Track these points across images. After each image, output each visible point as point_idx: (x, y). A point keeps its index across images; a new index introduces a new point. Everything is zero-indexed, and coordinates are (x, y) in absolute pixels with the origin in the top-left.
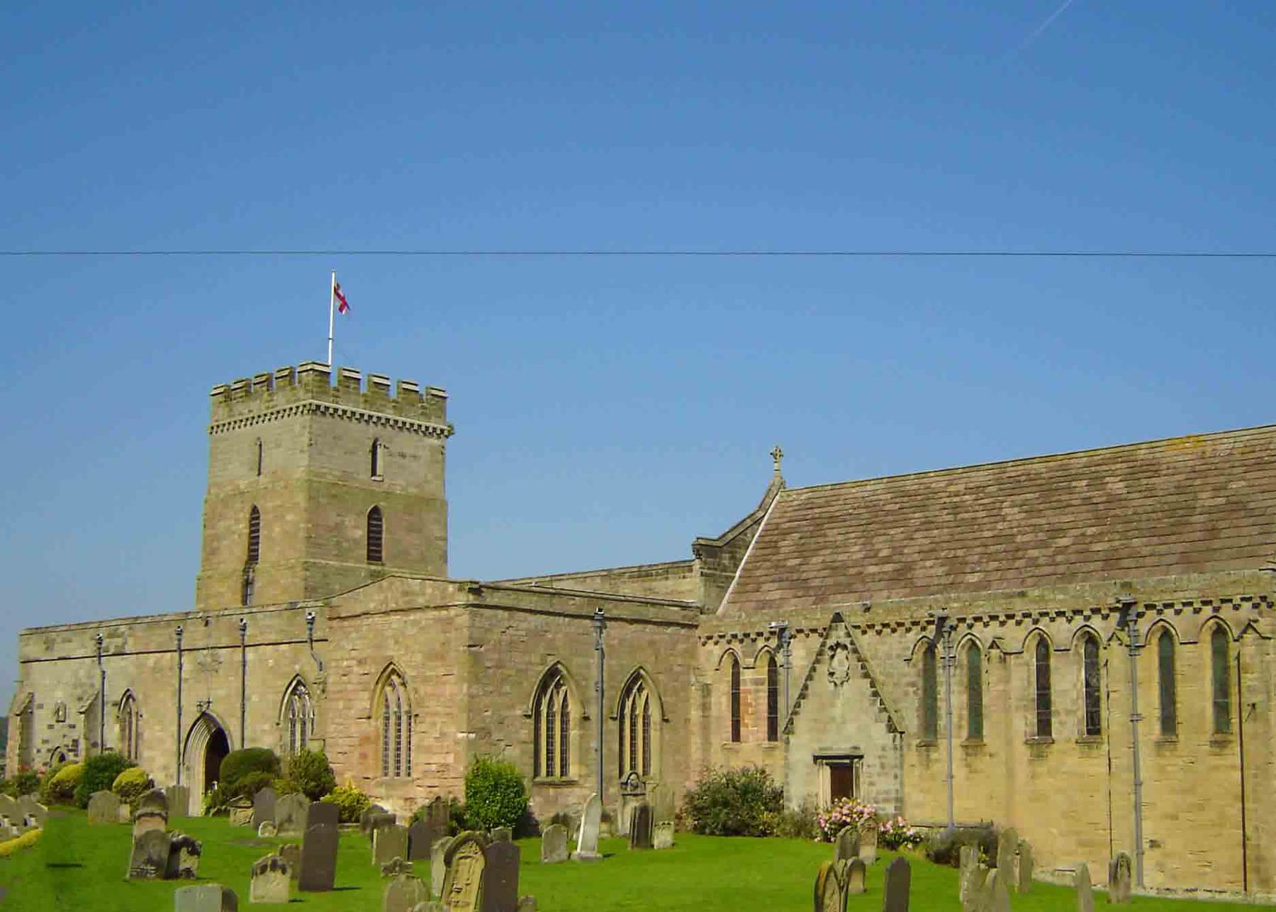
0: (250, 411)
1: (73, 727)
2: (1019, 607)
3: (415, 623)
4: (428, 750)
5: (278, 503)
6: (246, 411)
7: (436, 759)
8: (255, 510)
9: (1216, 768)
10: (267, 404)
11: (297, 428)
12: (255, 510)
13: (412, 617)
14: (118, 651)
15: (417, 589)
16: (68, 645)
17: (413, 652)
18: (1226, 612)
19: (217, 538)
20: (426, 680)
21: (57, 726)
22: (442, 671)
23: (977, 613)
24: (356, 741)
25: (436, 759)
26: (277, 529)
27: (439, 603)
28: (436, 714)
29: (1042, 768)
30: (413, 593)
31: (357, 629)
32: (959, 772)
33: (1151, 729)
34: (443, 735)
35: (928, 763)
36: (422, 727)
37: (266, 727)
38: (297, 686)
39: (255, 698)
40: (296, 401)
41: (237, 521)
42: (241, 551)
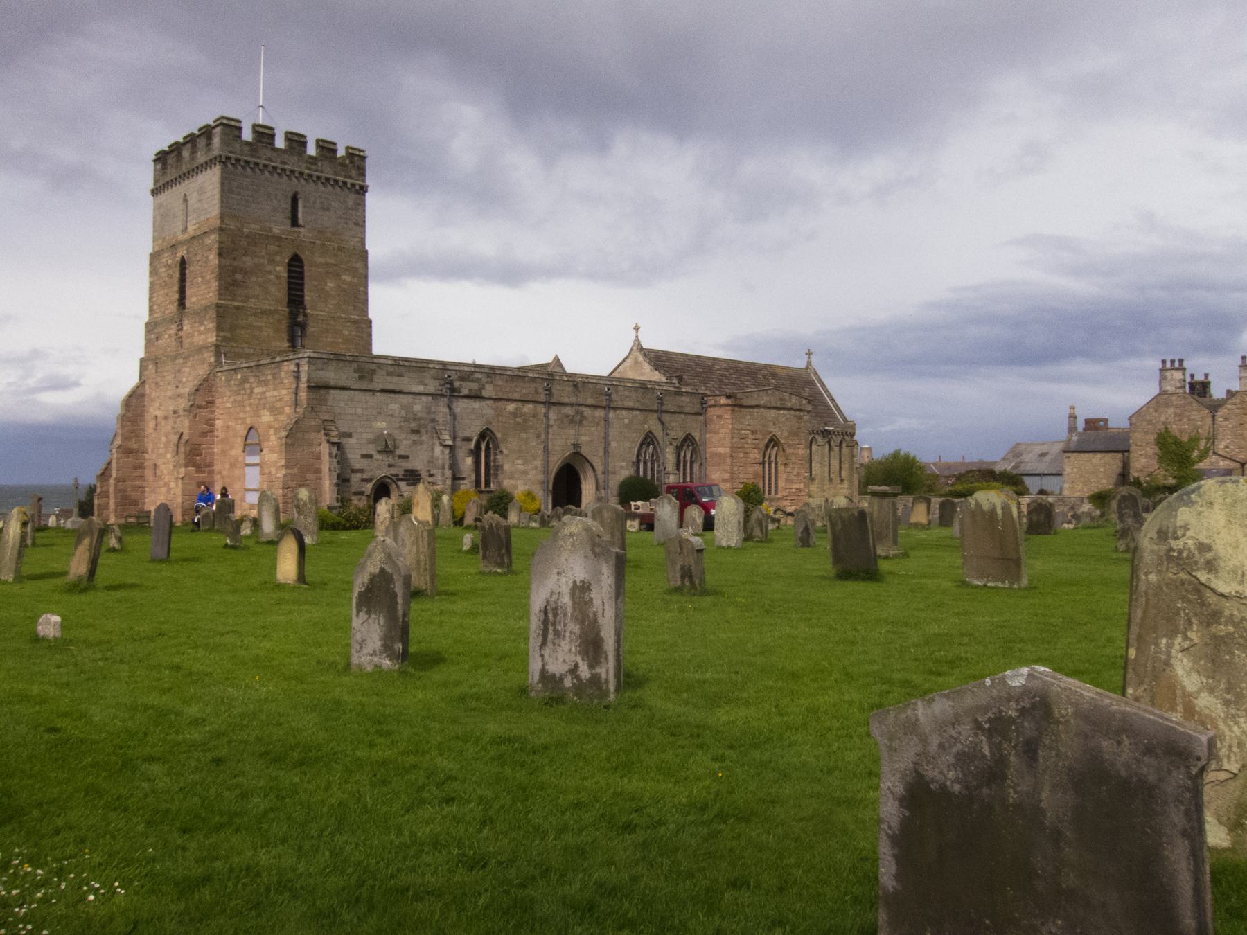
0: (283, 163)
1: (406, 457)
3: (784, 415)
5: (332, 261)
6: (279, 160)
10: (309, 166)
13: (782, 412)
14: (473, 394)
16: (395, 379)
19: (244, 271)
20: (789, 446)
21: (378, 457)
22: (797, 442)
25: (795, 486)
26: (329, 284)
28: (795, 463)
30: (785, 400)
34: (798, 474)
37: (624, 464)
38: (649, 439)
39: (614, 444)
40: (345, 177)
41: (272, 262)
42: (279, 291)
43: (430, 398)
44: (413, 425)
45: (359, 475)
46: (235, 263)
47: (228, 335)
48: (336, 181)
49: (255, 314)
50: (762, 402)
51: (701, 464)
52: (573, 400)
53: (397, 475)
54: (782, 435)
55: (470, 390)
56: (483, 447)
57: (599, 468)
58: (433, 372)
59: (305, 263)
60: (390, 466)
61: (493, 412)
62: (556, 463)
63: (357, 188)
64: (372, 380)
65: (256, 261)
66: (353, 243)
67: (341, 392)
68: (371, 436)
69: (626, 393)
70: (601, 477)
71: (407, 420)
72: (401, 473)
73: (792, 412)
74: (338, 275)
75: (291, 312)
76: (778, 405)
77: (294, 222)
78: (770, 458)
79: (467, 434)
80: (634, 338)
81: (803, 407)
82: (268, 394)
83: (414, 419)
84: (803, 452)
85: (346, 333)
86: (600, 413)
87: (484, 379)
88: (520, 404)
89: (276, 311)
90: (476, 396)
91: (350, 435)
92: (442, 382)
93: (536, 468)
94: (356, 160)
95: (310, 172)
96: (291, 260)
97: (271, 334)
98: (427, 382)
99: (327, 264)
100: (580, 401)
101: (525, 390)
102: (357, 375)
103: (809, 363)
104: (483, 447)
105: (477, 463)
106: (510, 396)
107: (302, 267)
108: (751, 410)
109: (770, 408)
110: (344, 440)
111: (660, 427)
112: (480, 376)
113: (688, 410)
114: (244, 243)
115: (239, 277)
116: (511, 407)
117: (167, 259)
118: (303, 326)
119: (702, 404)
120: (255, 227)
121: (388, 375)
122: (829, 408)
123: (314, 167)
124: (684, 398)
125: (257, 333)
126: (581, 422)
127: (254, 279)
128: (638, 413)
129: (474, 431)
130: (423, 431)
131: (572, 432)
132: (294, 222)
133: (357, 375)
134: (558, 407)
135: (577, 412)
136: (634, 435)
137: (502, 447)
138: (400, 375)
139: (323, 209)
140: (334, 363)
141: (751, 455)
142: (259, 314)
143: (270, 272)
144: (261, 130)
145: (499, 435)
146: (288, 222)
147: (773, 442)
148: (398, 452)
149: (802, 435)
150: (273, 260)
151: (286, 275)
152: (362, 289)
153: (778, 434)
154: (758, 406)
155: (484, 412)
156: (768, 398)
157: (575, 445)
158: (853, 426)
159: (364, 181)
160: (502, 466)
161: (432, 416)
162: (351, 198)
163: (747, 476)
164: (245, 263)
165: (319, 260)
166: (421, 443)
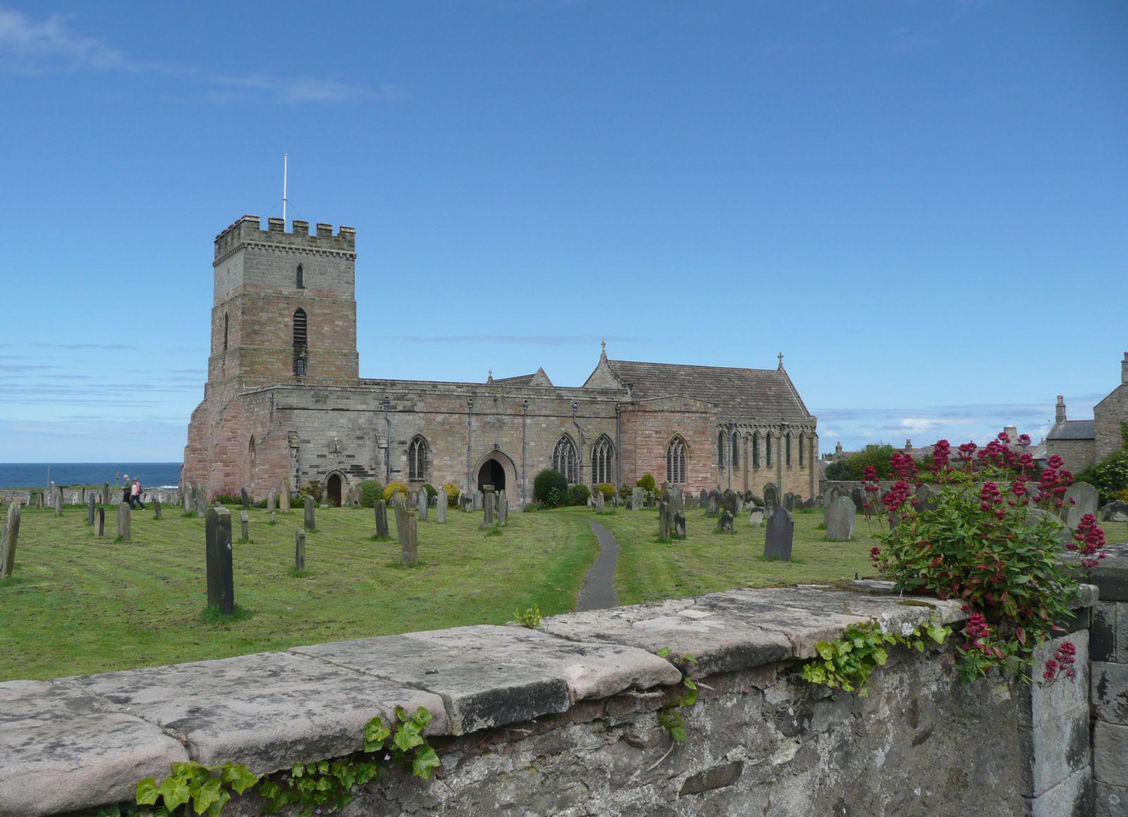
0: (290, 243)
1: (354, 456)
2: (753, 422)
3: (688, 418)
4: (697, 471)
5: (328, 311)
7: (701, 475)
8: (300, 312)
9: (802, 475)
11: (343, 268)
12: (300, 312)
13: (687, 415)
14: (406, 409)
15: (692, 404)
17: (688, 431)
18: (805, 430)
20: (695, 442)
21: (331, 456)
22: (703, 439)
23: (741, 423)
24: (656, 468)
25: (701, 475)
26: (326, 329)
27: (704, 410)
29: (756, 476)
30: (690, 405)
31: (655, 418)
32: (732, 477)
33: (784, 463)
34: (704, 465)
35: (722, 474)
36: (695, 462)
37: (542, 459)
38: (566, 439)
39: (532, 444)
40: (339, 249)
41: (282, 315)
42: (287, 335)
43: (372, 413)
44: (358, 433)
45: (315, 469)
46: (255, 318)
47: (249, 369)
48: (332, 253)
49: (269, 353)
50: (666, 408)
51: (617, 458)
52: (494, 411)
53: (345, 469)
54: (687, 435)
55: (404, 407)
56: (417, 447)
57: (518, 462)
58: (374, 395)
59: (308, 314)
60: (340, 463)
61: (424, 422)
62: (479, 458)
63: (348, 256)
64: (325, 402)
65: (270, 315)
66: (345, 296)
67: (302, 411)
68: (326, 442)
69: (543, 404)
70: (519, 469)
71: (353, 430)
72: (348, 468)
73: (697, 415)
74: (333, 322)
75: (295, 351)
76: (683, 409)
77: (300, 285)
78: (675, 453)
79: (402, 439)
80: (601, 352)
81: (708, 410)
82: (260, 413)
83: (359, 429)
84: (710, 447)
85: (338, 363)
86: (519, 420)
87: (416, 398)
88: (447, 415)
89: (284, 350)
90: (410, 411)
91: (308, 442)
92: (381, 402)
93: (461, 463)
94: (346, 237)
95: (310, 248)
96: (297, 312)
97: (281, 367)
98: (369, 402)
99: (325, 314)
100: (500, 411)
101: (455, 404)
102: (314, 400)
103: (780, 365)
104: (417, 447)
105: (411, 460)
106: (438, 410)
107: (305, 317)
108: (655, 414)
109: (674, 412)
110: (302, 446)
111: (576, 429)
112: (410, 396)
113: (603, 415)
114: (260, 303)
115: (256, 327)
116: (440, 418)
117: (220, 314)
118: (305, 359)
119: (617, 410)
120: (270, 291)
121: (338, 398)
122: (793, 403)
123: (314, 244)
124: (599, 406)
125: (269, 366)
126: (501, 427)
127: (268, 328)
128: (555, 418)
129: (408, 436)
130: (366, 437)
131: (493, 435)
132: (300, 285)
133: (314, 400)
134: (481, 416)
135: (499, 421)
136: (551, 436)
137: (432, 447)
138: (348, 398)
139: (321, 274)
140: (297, 391)
141: (655, 451)
142: (271, 353)
143: (280, 323)
144: (274, 222)
145: (429, 439)
146: (295, 285)
147: (679, 440)
148: (345, 453)
149: (709, 433)
150: (283, 314)
151: (292, 324)
152: (351, 330)
153: (683, 433)
154: (663, 411)
155: (417, 422)
156: (672, 405)
157: (496, 445)
158: (814, 420)
159: (353, 251)
160: (432, 462)
161: (374, 427)
162: (343, 264)
163: (651, 468)
164: (261, 317)
165: (317, 311)
166: (364, 446)
